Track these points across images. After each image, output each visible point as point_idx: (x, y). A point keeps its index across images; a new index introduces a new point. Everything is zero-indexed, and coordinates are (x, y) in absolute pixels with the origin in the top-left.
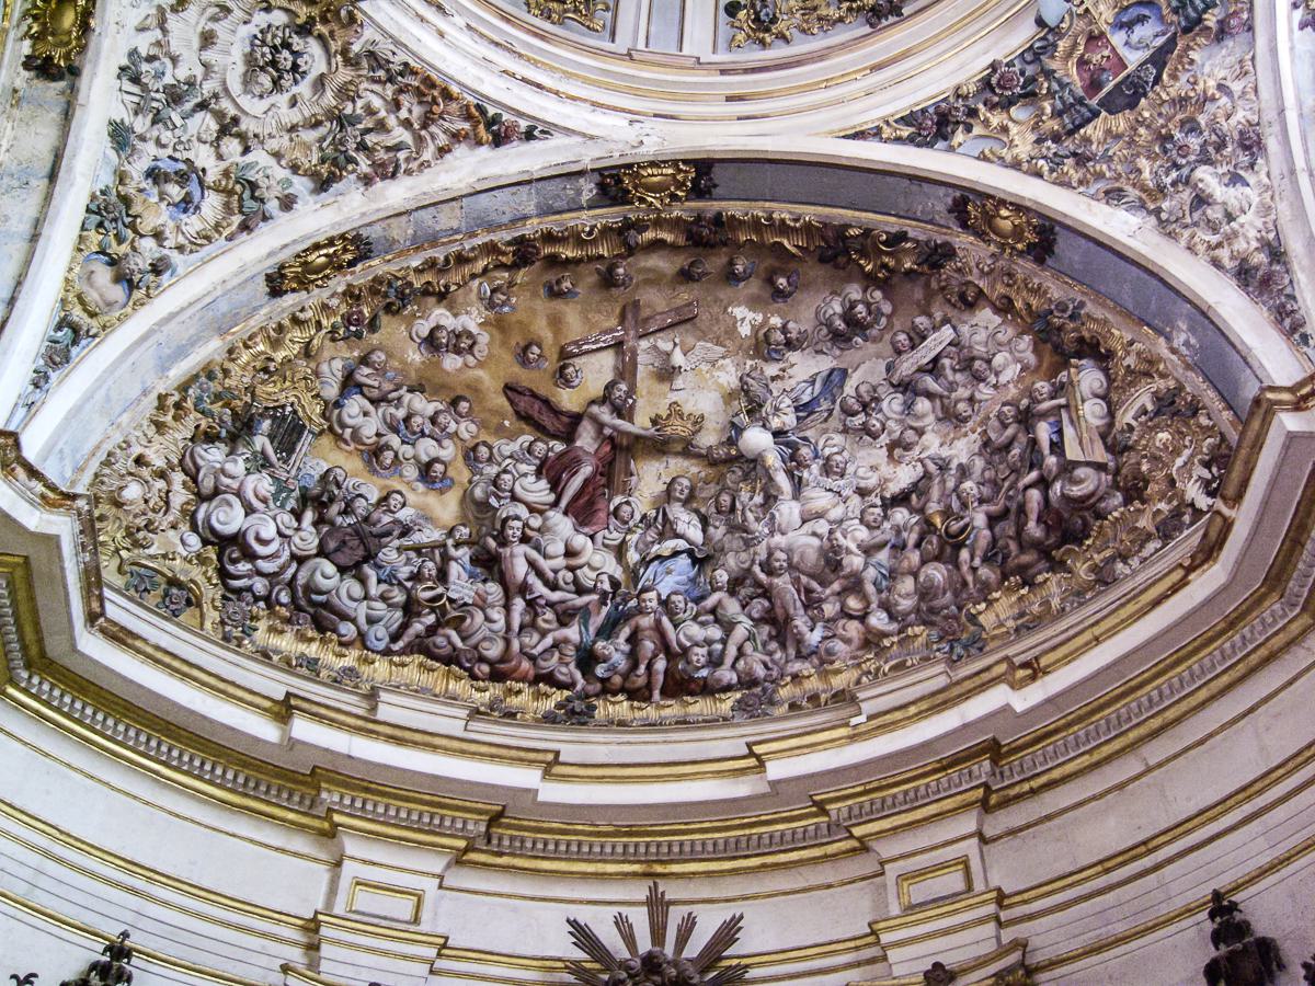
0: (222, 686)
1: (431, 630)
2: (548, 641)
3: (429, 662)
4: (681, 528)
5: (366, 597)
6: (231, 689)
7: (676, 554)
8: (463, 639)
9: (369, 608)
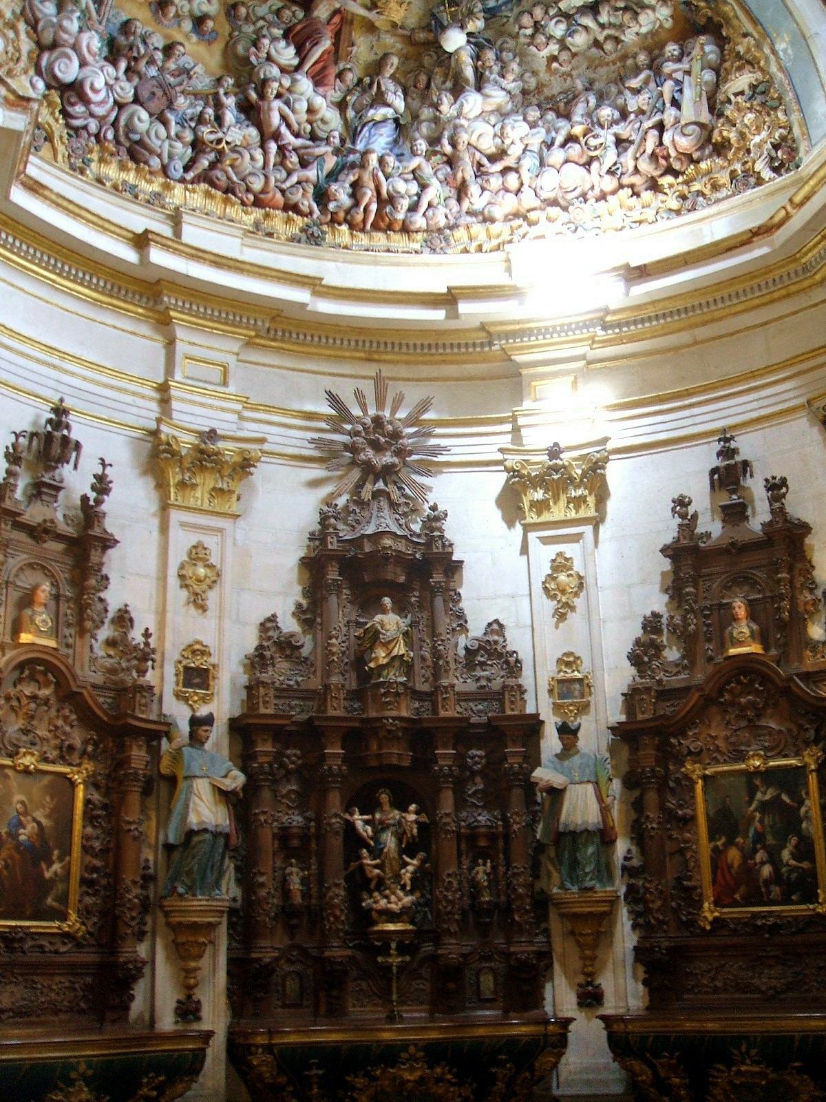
0: (101, 222)
1: (213, 166)
2: (294, 179)
3: (213, 191)
4: (390, 98)
5: (168, 137)
6: (107, 225)
7: (385, 120)
8: (236, 174)
9: (171, 146)
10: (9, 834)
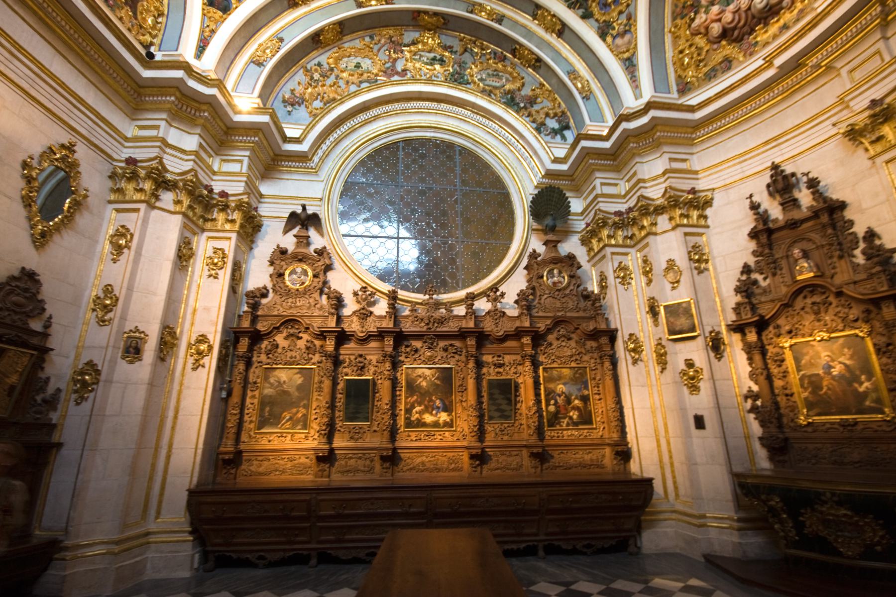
10: (825, 373)
